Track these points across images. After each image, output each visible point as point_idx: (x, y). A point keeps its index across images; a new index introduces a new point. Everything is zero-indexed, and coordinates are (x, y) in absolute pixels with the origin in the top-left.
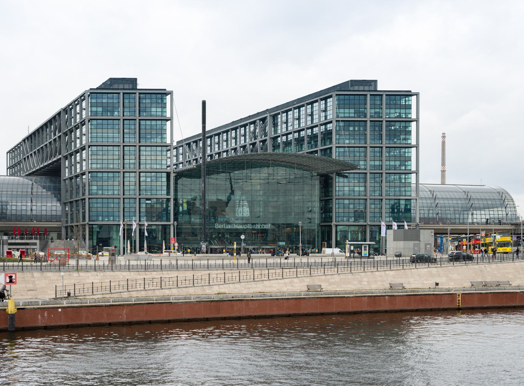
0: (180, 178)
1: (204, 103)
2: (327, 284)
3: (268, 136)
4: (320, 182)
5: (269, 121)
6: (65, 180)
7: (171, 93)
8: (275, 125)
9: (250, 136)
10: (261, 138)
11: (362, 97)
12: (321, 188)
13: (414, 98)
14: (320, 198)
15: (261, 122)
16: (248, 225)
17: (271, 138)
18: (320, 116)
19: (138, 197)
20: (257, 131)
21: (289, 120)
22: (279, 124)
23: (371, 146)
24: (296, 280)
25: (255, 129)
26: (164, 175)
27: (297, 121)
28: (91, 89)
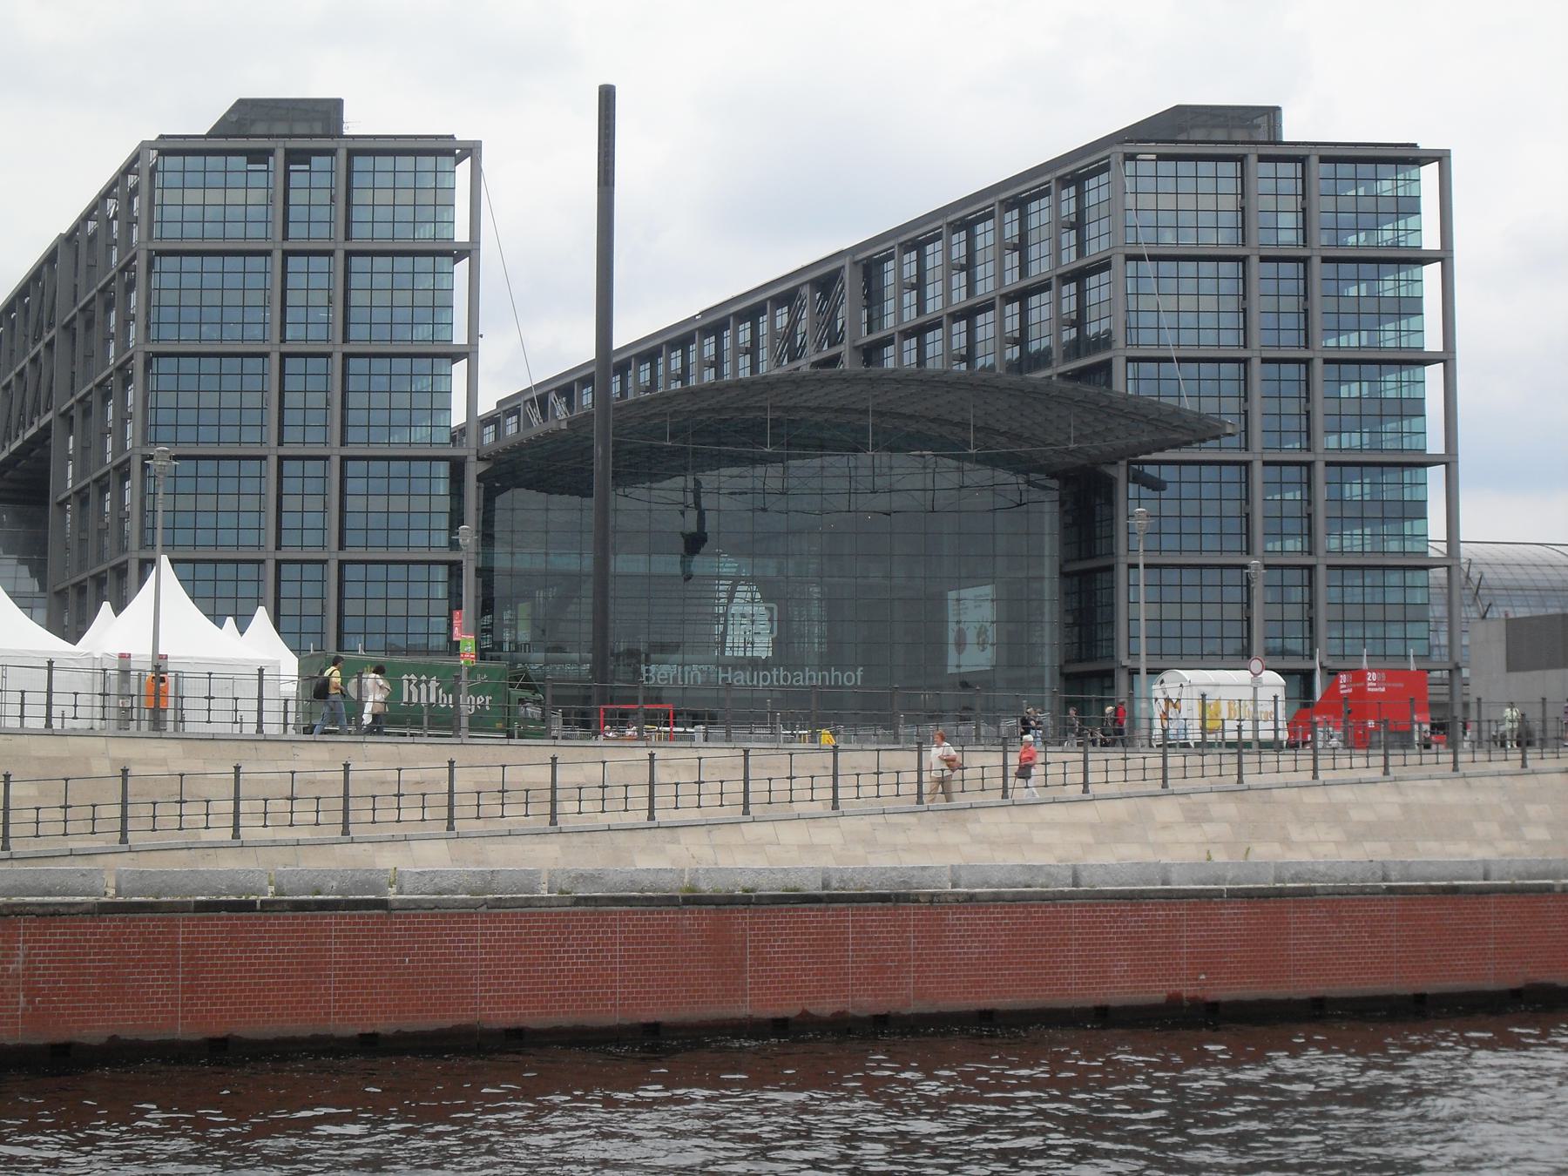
0: (504, 489)
1: (607, 96)
2: (1337, 835)
3: (846, 341)
4: (1062, 503)
5: (850, 284)
6: (62, 504)
7: (471, 151)
8: (872, 296)
9: (772, 349)
10: (819, 349)
11: (1229, 168)
12: (1065, 527)
13: (1429, 174)
14: (1061, 566)
15: (818, 295)
16: (775, 672)
17: (856, 348)
18: (1059, 242)
19: (334, 556)
20: (802, 327)
21: (929, 276)
22: (889, 292)
23: (1265, 355)
24: (1166, 810)
25: (793, 323)
26: (443, 469)
27: (964, 274)
28: (162, 137)
